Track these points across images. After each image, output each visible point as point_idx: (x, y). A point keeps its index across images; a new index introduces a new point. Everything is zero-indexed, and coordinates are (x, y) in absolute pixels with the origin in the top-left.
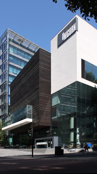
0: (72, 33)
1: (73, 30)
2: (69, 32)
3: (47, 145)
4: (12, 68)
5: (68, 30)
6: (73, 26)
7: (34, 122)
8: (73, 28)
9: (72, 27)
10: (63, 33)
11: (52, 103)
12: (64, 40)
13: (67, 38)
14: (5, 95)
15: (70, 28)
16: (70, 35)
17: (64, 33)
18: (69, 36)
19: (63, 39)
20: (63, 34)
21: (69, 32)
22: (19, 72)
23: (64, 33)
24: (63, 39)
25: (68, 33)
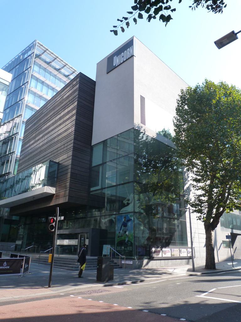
0: (127, 58)
1: (129, 55)
2: (123, 57)
3: (76, 246)
4: (35, 81)
5: (123, 53)
6: (129, 49)
7: (64, 164)
8: (130, 52)
9: (127, 50)
10: (115, 56)
11: (93, 161)
12: (117, 66)
13: (120, 63)
14: (13, 137)
15: (126, 51)
16: (125, 60)
17: (116, 56)
18: (123, 61)
19: (114, 65)
20: (114, 57)
21: (123, 57)
22: (42, 103)
23: (116, 56)
24: (114, 65)
25: (122, 57)
